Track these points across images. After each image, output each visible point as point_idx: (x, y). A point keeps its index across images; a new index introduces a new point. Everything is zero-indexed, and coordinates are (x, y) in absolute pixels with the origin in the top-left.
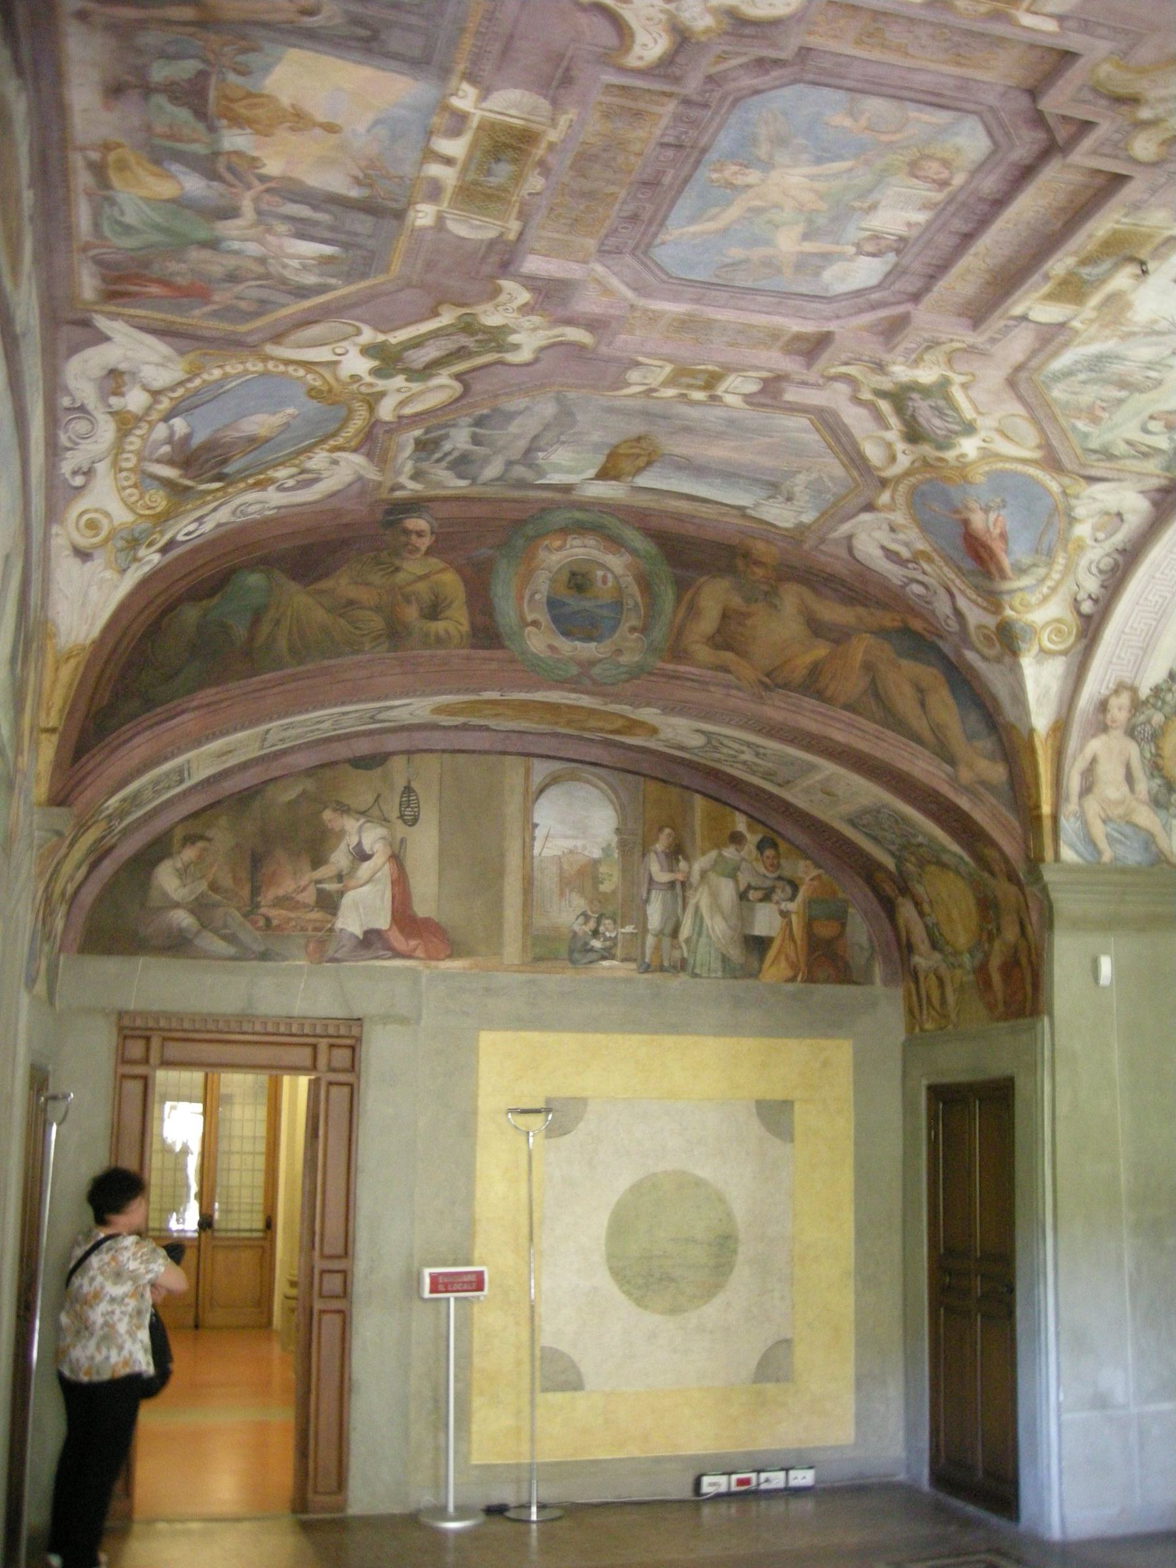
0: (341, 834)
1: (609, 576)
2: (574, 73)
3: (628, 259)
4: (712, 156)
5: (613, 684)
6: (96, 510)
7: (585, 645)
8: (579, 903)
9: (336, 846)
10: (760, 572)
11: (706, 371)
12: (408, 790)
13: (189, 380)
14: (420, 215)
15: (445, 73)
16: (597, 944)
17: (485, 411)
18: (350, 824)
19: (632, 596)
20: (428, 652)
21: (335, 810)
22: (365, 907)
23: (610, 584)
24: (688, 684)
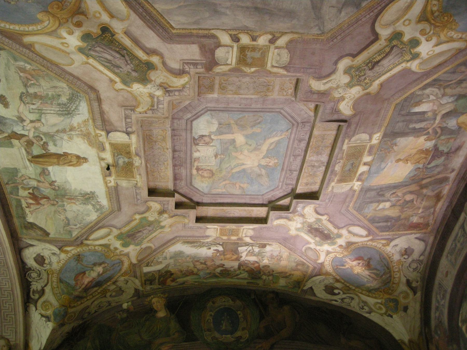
3: (299, 120)
4: (279, 168)
11: (250, 65)
14: (377, 138)
15: (361, 190)
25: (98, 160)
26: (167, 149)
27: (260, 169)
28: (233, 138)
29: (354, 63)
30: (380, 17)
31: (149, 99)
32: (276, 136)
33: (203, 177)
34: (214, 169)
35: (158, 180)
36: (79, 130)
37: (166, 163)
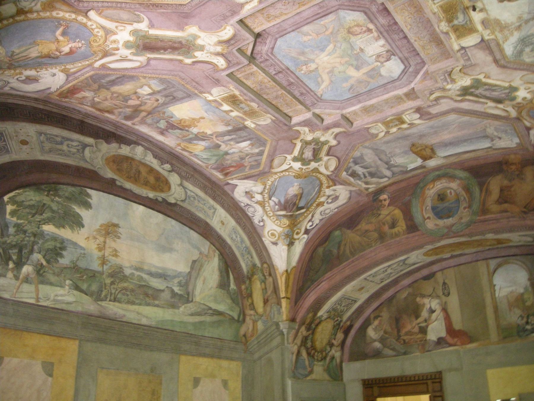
0: (424, 305)
1: (452, 191)
2: (216, 78)
5: (462, 231)
6: (271, 230)
7: (448, 220)
8: (518, 312)
9: (422, 310)
10: (513, 167)
12: (444, 284)
13: (265, 187)
16: (529, 327)
17: (352, 160)
18: (426, 301)
19: (463, 196)
20: (393, 241)
21: (420, 297)
22: (436, 330)
23: (453, 194)
24: (491, 222)
25: (487, 7)
26: (415, 41)
27: (308, 58)
28: (360, 71)
29: (327, 145)
30: (337, 160)
31: (454, 77)
32: (325, 88)
33: (358, 25)
34: (353, 39)
35: (406, 5)
36: (511, 30)
37: (409, 27)
